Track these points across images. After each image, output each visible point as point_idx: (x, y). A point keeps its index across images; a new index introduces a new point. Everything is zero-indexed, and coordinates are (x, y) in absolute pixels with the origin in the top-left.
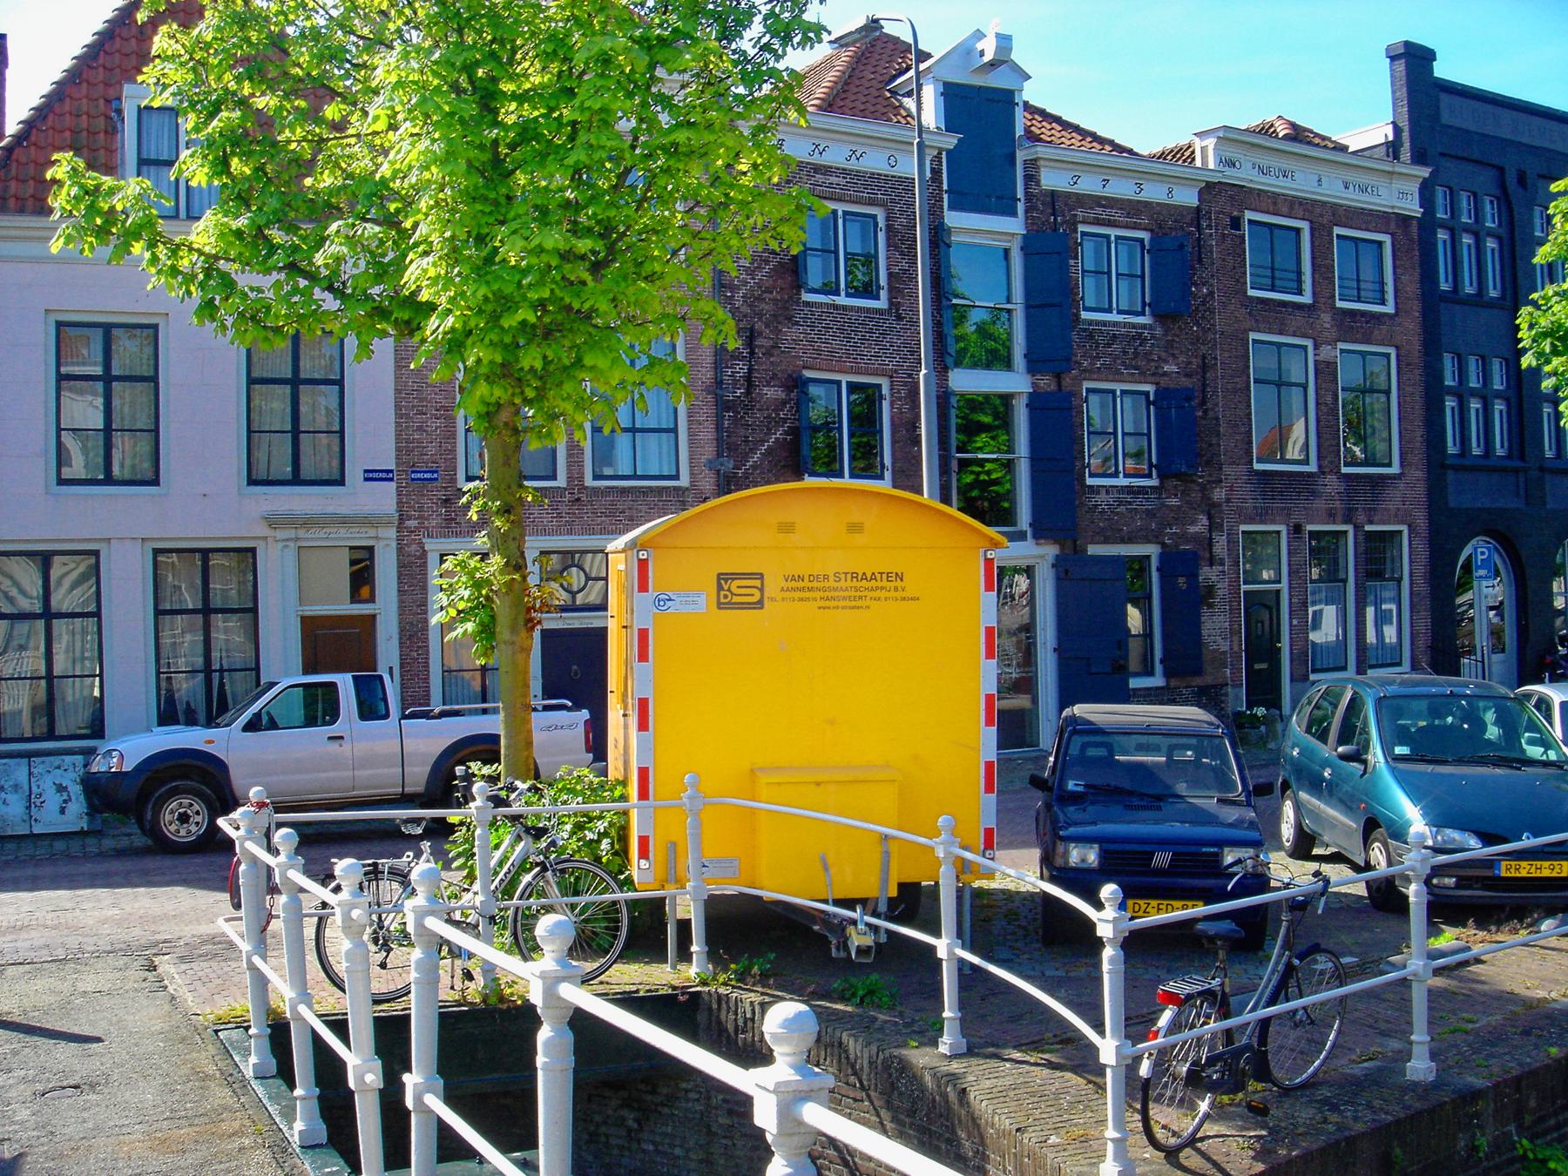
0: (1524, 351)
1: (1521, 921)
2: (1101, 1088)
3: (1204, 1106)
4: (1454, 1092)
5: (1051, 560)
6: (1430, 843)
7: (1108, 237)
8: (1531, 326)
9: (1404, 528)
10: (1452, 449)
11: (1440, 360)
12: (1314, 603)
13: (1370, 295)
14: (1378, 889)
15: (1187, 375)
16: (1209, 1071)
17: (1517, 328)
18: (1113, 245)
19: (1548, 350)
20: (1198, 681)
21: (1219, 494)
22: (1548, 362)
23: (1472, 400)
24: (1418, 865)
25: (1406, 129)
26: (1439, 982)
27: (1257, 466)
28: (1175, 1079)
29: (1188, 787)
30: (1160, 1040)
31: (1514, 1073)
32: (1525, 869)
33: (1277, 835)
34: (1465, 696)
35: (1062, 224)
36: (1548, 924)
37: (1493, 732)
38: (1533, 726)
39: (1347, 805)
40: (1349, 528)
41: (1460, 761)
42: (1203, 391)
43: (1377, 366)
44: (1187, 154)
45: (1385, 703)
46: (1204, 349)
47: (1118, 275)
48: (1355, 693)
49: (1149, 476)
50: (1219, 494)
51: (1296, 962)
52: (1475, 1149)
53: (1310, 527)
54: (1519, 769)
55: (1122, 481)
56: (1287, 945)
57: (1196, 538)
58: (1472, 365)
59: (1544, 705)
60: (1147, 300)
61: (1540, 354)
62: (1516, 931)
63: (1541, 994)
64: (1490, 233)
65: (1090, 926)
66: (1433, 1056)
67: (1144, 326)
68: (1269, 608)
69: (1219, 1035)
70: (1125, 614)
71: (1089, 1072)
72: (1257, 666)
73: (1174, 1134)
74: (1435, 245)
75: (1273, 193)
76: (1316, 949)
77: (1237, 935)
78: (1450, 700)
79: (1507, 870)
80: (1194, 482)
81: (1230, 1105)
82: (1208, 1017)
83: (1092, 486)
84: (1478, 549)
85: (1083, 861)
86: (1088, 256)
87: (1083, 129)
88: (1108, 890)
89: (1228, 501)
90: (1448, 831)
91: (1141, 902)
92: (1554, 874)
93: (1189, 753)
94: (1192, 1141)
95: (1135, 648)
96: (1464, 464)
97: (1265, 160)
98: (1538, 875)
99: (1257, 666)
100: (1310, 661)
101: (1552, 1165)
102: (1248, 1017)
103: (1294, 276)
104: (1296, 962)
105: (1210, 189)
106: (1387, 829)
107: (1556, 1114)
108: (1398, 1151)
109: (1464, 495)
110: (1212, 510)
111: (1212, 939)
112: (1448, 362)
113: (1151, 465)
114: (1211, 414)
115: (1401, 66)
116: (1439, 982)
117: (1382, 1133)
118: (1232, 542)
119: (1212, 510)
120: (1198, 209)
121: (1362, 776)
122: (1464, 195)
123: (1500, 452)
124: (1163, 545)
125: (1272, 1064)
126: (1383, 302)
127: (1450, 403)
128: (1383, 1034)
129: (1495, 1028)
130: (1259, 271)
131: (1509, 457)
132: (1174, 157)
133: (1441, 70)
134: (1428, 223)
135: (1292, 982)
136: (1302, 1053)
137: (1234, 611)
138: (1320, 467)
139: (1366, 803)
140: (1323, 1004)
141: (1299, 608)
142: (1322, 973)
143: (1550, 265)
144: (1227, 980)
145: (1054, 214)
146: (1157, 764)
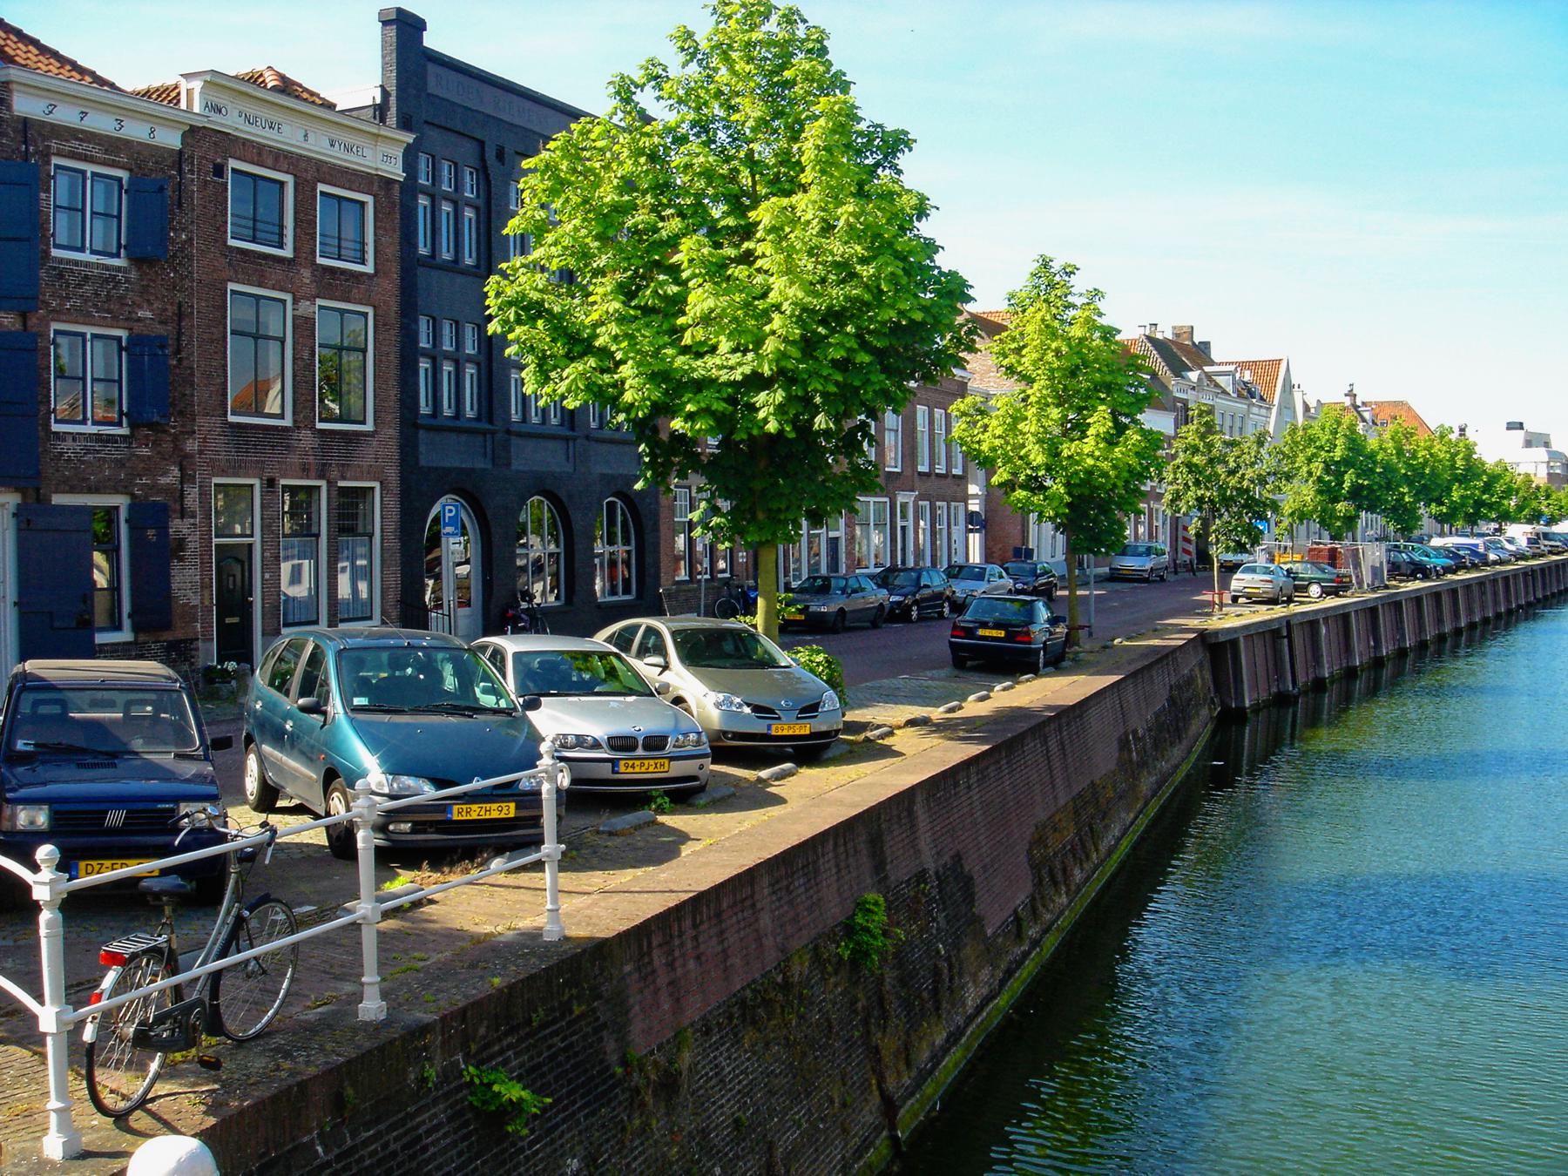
0: (490, 318)
1: (472, 861)
2: (43, 1056)
3: (154, 1066)
4: (402, 1028)
5: (12, 508)
6: (386, 790)
7: (83, 173)
8: (498, 295)
9: (376, 485)
10: (424, 409)
11: (416, 321)
12: (287, 558)
13: (352, 253)
14: (338, 837)
15: (161, 322)
16: (158, 1030)
17: (486, 296)
18: (89, 182)
19: (512, 318)
20: (167, 636)
21: (191, 446)
22: (512, 330)
23: (468, 365)
24: (365, 811)
25: (394, 94)
26: (391, 924)
27: (231, 419)
28: (121, 1041)
29: (147, 743)
30: (104, 1003)
31: (460, 1005)
32: (476, 812)
33: (241, 789)
34: (424, 648)
35: (33, 155)
36: (497, 863)
37: (450, 683)
38: (486, 678)
39: (308, 757)
40: (323, 483)
41: (416, 711)
42: (178, 339)
43: (355, 325)
44: (173, 94)
45: (345, 654)
46: (179, 297)
47: (93, 213)
48: (317, 647)
49: (120, 424)
50: (191, 446)
51: (246, 913)
52: (424, 1080)
53: (283, 482)
54: (471, 717)
55: (90, 429)
56: (238, 897)
57: (167, 490)
58: (447, 330)
59: (498, 656)
60: (123, 242)
61: (506, 322)
62: (467, 871)
63: (488, 929)
64: (469, 204)
65: (26, 888)
66: (384, 995)
67: (119, 269)
68: (241, 562)
69: (168, 992)
70: (91, 565)
71: (35, 1043)
72: (228, 620)
73: (124, 1097)
74: (416, 208)
75: (258, 143)
76: (266, 899)
77: (182, 890)
78: (408, 651)
79: (459, 813)
80: (165, 432)
81: (183, 1062)
82: (156, 975)
83: (57, 433)
84: (446, 507)
85: (32, 823)
86: (61, 190)
87: (62, 57)
88: (45, 852)
89: (201, 452)
90: (404, 778)
91: (94, 863)
92: (502, 816)
93: (149, 708)
94: (142, 1103)
95: (101, 604)
96: (436, 425)
97: (252, 109)
98: (488, 817)
99: (228, 620)
100: (283, 614)
101: (496, 1088)
102: (196, 971)
103: (276, 230)
104: (246, 913)
105: (193, 133)
106: (345, 779)
107: (499, 1040)
108: (350, 1091)
109: (436, 454)
110: (184, 462)
111: (157, 896)
112: (423, 325)
113: (121, 413)
114: (185, 363)
115: (392, 31)
116: (391, 924)
117: (334, 1074)
118: (204, 495)
119: (184, 462)
120: (181, 152)
121: (322, 727)
122: (446, 165)
123: (469, 413)
124: (133, 496)
125: (225, 1018)
126: (363, 262)
127: (424, 365)
128: (337, 978)
129: (444, 964)
130: (237, 220)
131: (478, 419)
132: (159, 96)
133: (430, 40)
134: (410, 188)
135: (243, 934)
136: (256, 1003)
137: (205, 565)
138: (295, 421)
139: (326, 754)
140: (274, 954)
141: (272, 564)
142: (274, 922)
143: (522, 235)
144: (174, 936)
145: (25, 143)
146: (114, 722)
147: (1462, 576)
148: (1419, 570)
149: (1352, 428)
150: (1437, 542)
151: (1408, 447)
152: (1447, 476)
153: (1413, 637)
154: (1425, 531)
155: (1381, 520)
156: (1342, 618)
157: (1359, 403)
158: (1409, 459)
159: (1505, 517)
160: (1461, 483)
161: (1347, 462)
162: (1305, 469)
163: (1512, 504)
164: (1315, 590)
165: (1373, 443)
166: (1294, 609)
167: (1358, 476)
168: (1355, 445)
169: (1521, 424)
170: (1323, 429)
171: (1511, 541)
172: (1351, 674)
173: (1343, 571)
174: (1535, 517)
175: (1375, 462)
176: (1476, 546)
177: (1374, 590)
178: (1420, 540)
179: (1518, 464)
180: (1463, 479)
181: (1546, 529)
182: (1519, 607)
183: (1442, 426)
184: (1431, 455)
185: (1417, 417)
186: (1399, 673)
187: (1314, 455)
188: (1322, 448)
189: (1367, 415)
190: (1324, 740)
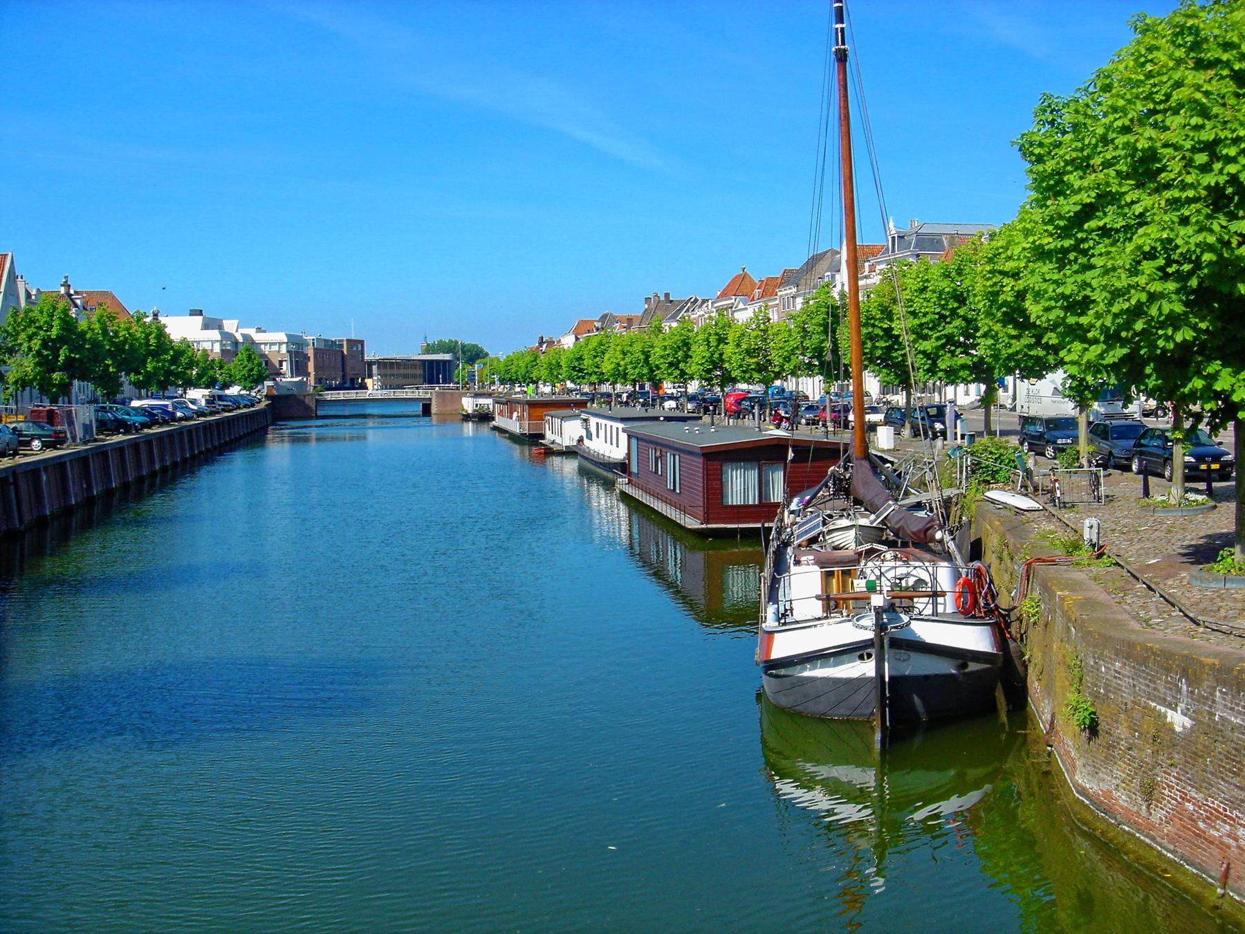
147: (156, 430)
148: (121, 426)
149: (66, 312)
150: (136, 403)
151: (111, 328)
152: (143, 351)
153: (118, 480)
154: (126, 395)
155: (91, 387)
156: (58, 465)
157: (72, 292)
158: (112, 337)
159: (190, 383)
160: (153, 356)
161: (61, 340)
162: (26, 345)
163: (194, 373)
164: (36, 444)
165: (83, 325)
166: (20, 460)
167: (71, 351)
168: (68, 325)
169: (201, 311)
170: (42, 312)
171: (194, 402)
172: (68, 511)
173: (59, 428)
174: (211, 384)
175: (85, 340)
176: (167, 406)
177: (85, 443)
178: (123, 403)
179: (198, 342)
180: (155, 354)
181: (220, 393)
182: (201, 453)
183: (138, 311)
184: (130, 334)
185: (120, 305)
186: (107, 511)
187: (35, 334)
188: (40, 328)
189: (78, 302)
190: (49, 566)
